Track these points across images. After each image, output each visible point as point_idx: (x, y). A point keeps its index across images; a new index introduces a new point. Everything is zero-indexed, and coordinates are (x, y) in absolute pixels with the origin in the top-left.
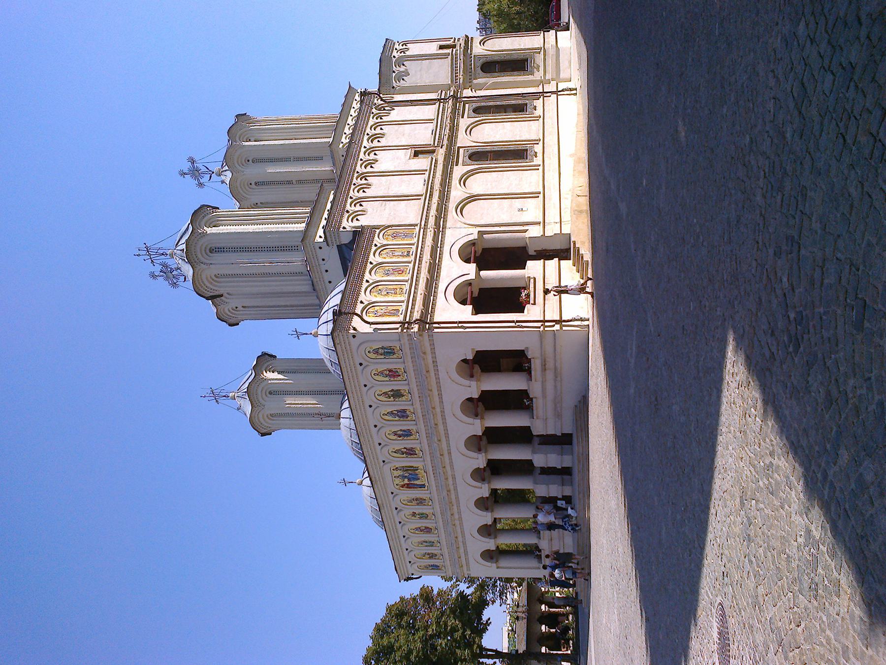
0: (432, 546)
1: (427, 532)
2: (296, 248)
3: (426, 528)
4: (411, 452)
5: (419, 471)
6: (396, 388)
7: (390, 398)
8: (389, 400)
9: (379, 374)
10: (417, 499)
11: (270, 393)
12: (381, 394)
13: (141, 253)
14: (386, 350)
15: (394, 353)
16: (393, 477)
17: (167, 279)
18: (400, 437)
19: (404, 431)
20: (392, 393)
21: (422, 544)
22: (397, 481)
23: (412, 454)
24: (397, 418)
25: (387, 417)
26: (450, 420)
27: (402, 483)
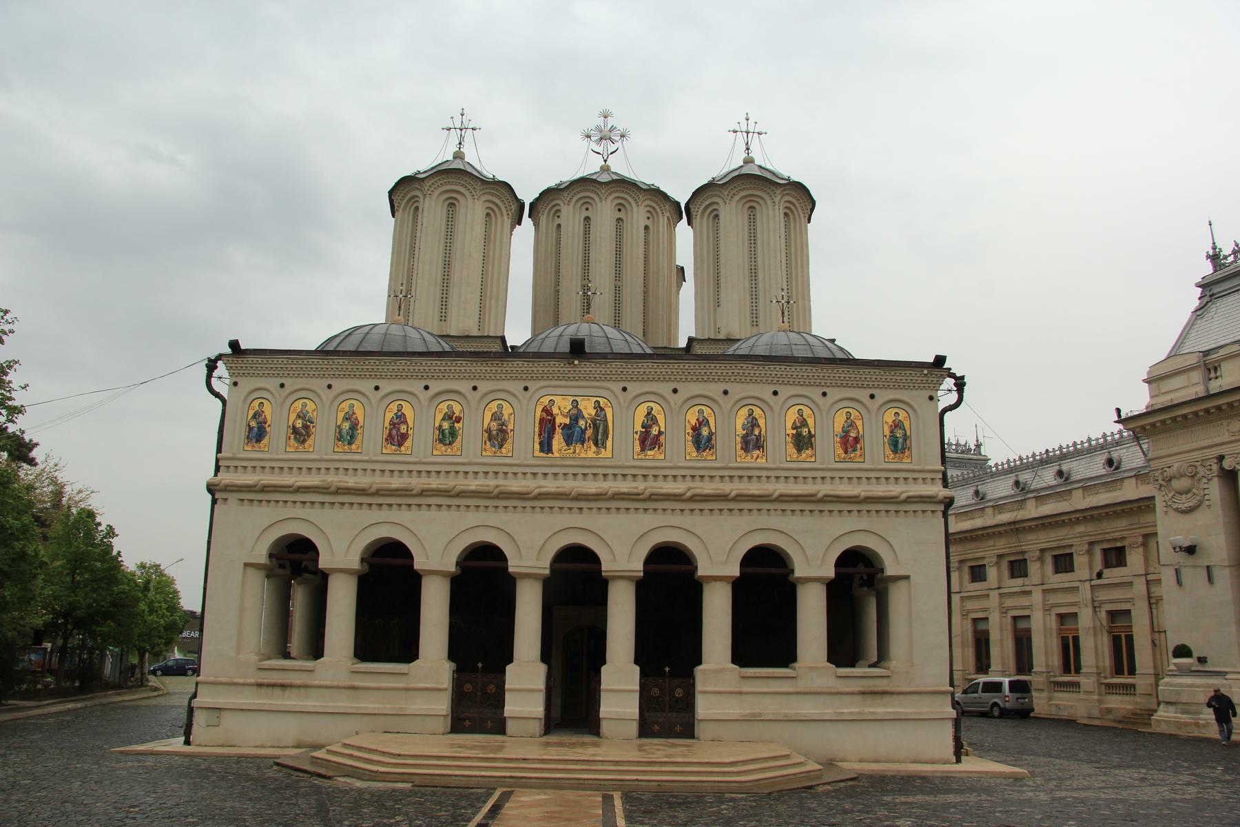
1: (390, 435)
2: (755, 323)
3: (404, 437)
4: (648, 442)
5: (594, 448)
6: (818, 442)
7: (793, 429)
8: (789, 424)
9: (849, 421)
10: (502, 431)
11: (488, 215)
12: (802, 416)
13: (751, 122)
14: (900, 441)
15: (895, 451)
16: (576, 398)
17: (599, 129)
18: (694, 429)
19: (709, 439)
20: (805, 431)
21: (346, 419)
23: (643, 442)
24: (741, 432)
25: (744, 412)
26: (745, 522)
27: (555, 411)
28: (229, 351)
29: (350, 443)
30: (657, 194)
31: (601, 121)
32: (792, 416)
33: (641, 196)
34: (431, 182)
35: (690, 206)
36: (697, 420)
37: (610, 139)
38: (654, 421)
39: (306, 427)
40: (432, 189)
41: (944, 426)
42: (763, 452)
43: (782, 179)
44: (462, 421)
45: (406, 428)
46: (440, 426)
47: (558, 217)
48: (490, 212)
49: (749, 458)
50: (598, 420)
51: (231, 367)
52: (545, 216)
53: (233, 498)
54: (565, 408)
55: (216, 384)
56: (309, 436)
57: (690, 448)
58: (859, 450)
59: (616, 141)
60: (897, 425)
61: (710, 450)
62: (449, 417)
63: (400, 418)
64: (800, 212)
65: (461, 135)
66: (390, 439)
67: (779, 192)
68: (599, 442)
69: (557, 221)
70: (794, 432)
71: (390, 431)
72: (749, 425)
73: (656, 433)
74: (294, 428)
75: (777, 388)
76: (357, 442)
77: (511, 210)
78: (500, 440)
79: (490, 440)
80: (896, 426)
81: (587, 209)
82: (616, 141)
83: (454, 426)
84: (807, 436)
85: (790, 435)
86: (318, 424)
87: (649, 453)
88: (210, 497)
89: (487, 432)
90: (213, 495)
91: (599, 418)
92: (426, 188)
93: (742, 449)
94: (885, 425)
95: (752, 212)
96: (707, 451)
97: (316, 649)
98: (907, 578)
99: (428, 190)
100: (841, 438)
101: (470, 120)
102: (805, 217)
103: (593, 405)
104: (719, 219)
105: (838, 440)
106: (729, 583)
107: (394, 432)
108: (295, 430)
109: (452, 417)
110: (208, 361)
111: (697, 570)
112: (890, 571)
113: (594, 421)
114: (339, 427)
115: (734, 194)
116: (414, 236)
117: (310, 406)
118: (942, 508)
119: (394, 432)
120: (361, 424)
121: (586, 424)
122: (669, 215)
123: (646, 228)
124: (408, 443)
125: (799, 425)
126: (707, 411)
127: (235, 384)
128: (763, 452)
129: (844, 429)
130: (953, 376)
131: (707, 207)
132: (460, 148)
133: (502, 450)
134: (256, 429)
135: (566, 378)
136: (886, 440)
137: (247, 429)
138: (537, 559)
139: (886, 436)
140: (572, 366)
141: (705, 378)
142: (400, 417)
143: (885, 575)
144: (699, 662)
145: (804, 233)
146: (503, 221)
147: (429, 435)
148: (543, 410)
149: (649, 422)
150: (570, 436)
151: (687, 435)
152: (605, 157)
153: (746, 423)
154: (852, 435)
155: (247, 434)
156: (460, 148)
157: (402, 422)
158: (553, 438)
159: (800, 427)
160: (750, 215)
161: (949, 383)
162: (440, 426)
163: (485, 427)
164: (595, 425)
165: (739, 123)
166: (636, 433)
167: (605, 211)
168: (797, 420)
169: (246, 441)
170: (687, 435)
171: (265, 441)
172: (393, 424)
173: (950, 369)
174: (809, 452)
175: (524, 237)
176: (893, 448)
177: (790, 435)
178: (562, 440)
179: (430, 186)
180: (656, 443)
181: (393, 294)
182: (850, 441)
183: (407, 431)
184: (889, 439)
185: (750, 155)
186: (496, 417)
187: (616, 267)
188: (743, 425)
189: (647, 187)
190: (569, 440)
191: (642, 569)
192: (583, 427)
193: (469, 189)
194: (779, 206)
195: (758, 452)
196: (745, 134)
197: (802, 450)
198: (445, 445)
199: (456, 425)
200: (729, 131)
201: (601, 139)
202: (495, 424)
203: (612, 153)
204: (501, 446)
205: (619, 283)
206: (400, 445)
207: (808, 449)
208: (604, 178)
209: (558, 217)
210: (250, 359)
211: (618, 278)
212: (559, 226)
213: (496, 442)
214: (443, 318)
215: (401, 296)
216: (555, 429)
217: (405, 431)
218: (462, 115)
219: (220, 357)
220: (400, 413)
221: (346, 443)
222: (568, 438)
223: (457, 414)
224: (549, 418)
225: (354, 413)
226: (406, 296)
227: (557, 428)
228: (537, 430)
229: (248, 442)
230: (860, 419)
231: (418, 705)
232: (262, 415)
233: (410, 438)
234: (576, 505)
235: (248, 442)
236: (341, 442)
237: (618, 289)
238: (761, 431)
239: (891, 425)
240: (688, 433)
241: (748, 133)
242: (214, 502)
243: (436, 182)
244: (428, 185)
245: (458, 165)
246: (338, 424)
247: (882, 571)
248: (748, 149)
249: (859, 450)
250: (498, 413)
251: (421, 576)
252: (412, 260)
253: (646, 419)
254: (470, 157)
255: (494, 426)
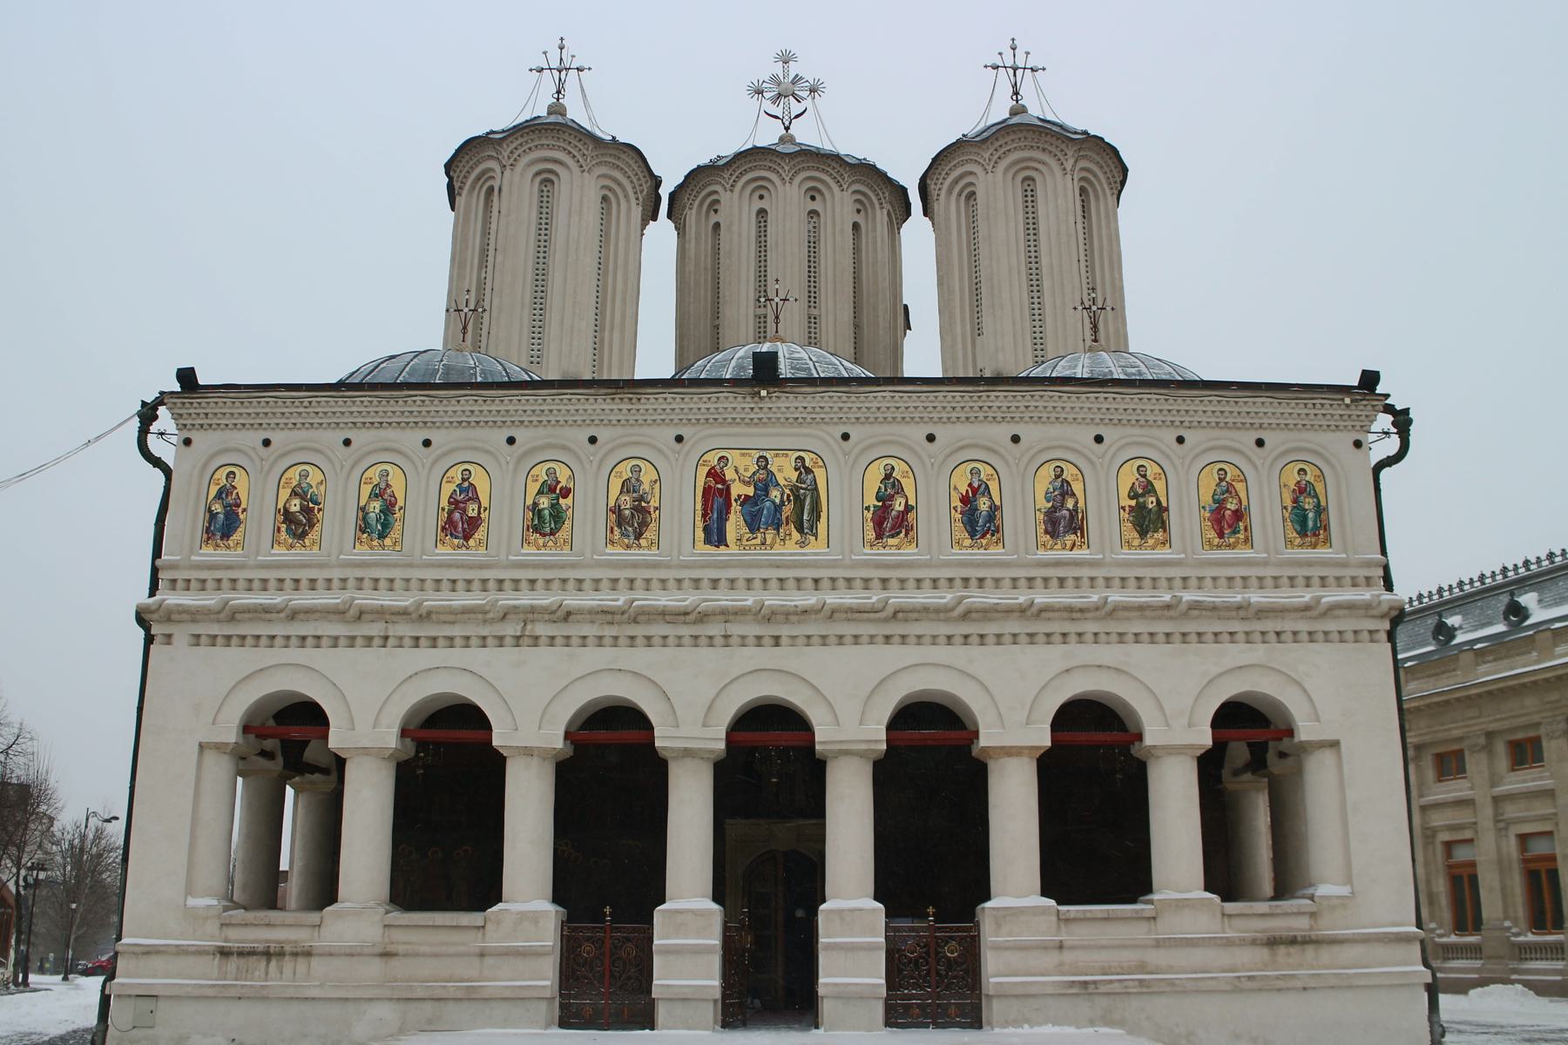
0: (364, 527)
1: (450, 520)
3: (474, 523)
4: (888, 525)
5: (796, 535)
6: (1173, 518)
7: (1131, 498)
8: (1124, 491)
9: (1224, 484)
11: (605, 199)
12: (1144, 476)
14: (1311, 515)
15: (1303, 533)
17: (775, 80)
18: (965, 500)
20: (1151, 502)
21: (377, 494)
22: (748, 465)
23: (879, 523)
25: (1048, 472)
26: (1054, 656)
27: (729, 474)
28: (177, 387)
29: (382, 536)
30: (868, 172)
31: (778, 69)
32: (1129, 477)
33: (846, 176)
34: (512, 146)
35: (928, 181)
36: (970, 485)
37: (793, 95)
38: (898, 488)
39: (306, 511)
40: (515, 156)
41: (1380, 490)
42: (1082, 536)
43: (1076, 133)
44: (571, 495)
45: (476, 509)
46: (535, 504)
47: (716, 211)
48: (607, 192)
49: (1059, 546)
50: (802, 488)
51: (181, 415)
52: (694, 211)
53: (181, 633)
54: (746, 470)
55: (154, 445)
56: (312, 526)
57: (961, 533)
58: (1242, 532)
59: (804, 99)
60: (1302, 490)
61: (992, 535)
62: (549, 488)
63: (467, 491)
64: (1106, 186)
65: (560, 79)
66: (449, 527)
67: (1072, 152)
68: (806, 525)
69: (713, 219)
70: (1133, 503)
71: (450, 513)
72: (1056, 493)
73: (902, 508)
74: (286, 510)
75: (1101, 431)
76: (395, 534)
77: (642, 192)
78: (636, 525)
79: (619, 526)
80: (1302, 491)
81: (761, 197)
82: (804, 99)
83: (558, 503)
84: (1156, 509)
85: (1127, 509)
86: (328, 505)
87: (891, 541)
88: (141, 633)
89: (614, 513)
90: (147, 629)
91: (803, 486)
92: (506, 154)
93: (1046, 532)
94: (1284, 490)
95: (1029, 185)
96: (988, 536)
97: (325, 890)
98: (1335, 744)
99: (509, 158)
100: (1212, 512)
101: (573, 56)
102: (1113, 194)
103: (793, 465)
104: (975, 200)
105: (1208, 515)
106: (1031, 758)
107: (457, 515)
108: (288, 517)
109: (556, 488)
110: (142, 407)
111: (977, 738)
112: (1305, 731)
113: (795, 490)
114: (363, 509)
115: (999, 158)
116: (486, 233)
117: (314, 477)
118: (1387, 626)
119: (457, 515)
120: (400, 503)
121: (782, 495)
122: (889, 207)
123: (856, 226)
124: (480, 534)
125: (1140, 491)
126: (985, 471)
127: (187, 442)
128: (1082, 536)
129: (1216, 497)
130: (1389, 409)
131: (956, 181)
132: (558, 99)
133: (641, 541)
134: (222, 516)
135: (747, 421)
136: (1287, 515)
137: (207, 515)
138: (704, 725)
139: (1286, 508)
140: (756, 399)
141: (981, 415)
142: (467, 490)
143: (1296, 740)
144: (984, 892)
145: (1112, 219)
146: (629, 209)
147: (519, 518)
148: (708, 475)
149: (889, 490)
150: (756, 515)
151: (953, 511)
152: (787, 123)
153: (1052, 490)
154: (1229, 506)
155: (206, 524)
156: (558, 99)
157: (470, 499)
158: (727, 520)
159: (1143, 495)
160: (1026, 191)
161: (1384, 421)
162: (535, 504)
163: (611, 503)
164: (797, 497)
165: (1000, 54)
166: (868, 508)
167: (788, 199)
168: (1137, 483)
169: (205, 536)
170: (953, 511)
171: (237, 536)
172: (454, 502)
173: (1387, 396)
174: (1159, 535)
175: (661, 237)
176: (1299, 529)
177: (1127, 509)
178: (742, 523)
179: (512, 152)
180: (901, 526)
181: (453, 309)
182: (1227, 516)
183: (479, 513)
184: (1290, 514)
185: (1020, 102)
186: (626, 487)
187: (809, 286)
188: (1046, 493)
189: (857, 162)
190: (753, 524)
191: (885, 738)
192: (777, 501)
193: (574, 156)
194: (1073, 175)
195: (1073, 537)
196: (1011, 72)
197: (1147, 532)
198: (544, 535)
199: (562, 501)
200: (986, 67)
201: (780, 95)
202: (628, 498)
203: (797, 116)
204: (638, 536)
205: (815, 312)
206: (467, 537)
207: (1157, 531)
208: (791, 149)
209: (716, 211)
210: (213, 399)
211: (812, 304)
212: (717, 226)
213: (630, 529)
214: (537, 359)
215: (466, 310)
216: (731, 503)
217: (472, 513)
218: (561, 48)
219: (161, 400)
220: (466, 484)
221: (375, 536)
222: (753, 520)
223: (563, 484)
224: (720, 486)
225: (388, 486)
226: (475, 310)
227: (734, 504)
228: (699, 506)
229: (208, 539)
230: (1241, 481)
231: (504, 979)
232: (232, 493)
233: (485, 525)
234: (768, 631)
235: (208, 539)
236: (366, 535)
237: (813, 320)
238: (1077, 502)
239: (1294, 489)
240: (955, 508)
241: (1015, 69)
242: (149, 640)
243: (521, 145)
244: (510, 149)
245: (560, 119)
246: (362, 503)
247: (1290, 732)
248: (1016, 93)
249: (1242, 532)
250: (633, 480)
251: (505, 758)
252: (484, 271)
253: (883, 486)
254: (576, 113)
255: (627, 501)
